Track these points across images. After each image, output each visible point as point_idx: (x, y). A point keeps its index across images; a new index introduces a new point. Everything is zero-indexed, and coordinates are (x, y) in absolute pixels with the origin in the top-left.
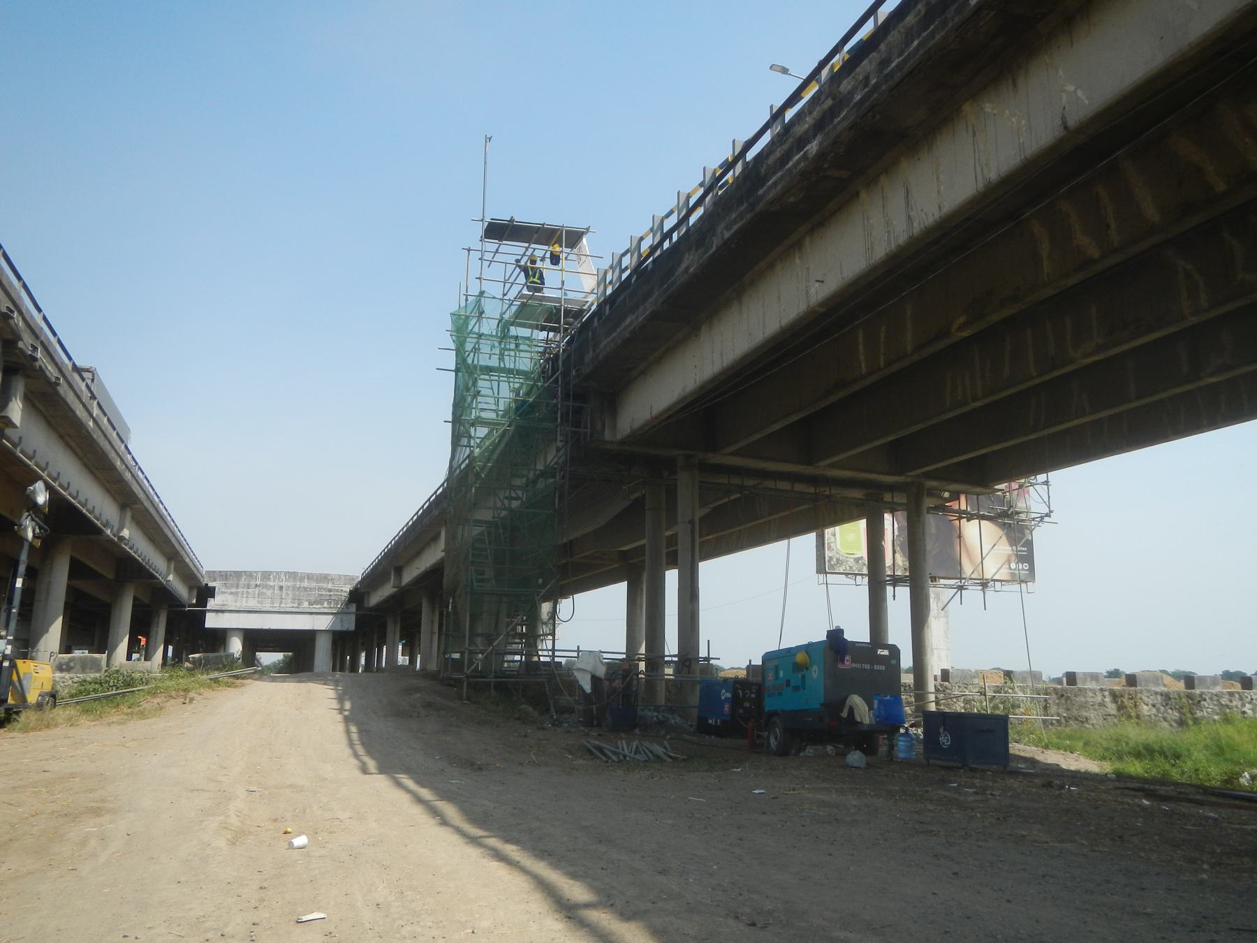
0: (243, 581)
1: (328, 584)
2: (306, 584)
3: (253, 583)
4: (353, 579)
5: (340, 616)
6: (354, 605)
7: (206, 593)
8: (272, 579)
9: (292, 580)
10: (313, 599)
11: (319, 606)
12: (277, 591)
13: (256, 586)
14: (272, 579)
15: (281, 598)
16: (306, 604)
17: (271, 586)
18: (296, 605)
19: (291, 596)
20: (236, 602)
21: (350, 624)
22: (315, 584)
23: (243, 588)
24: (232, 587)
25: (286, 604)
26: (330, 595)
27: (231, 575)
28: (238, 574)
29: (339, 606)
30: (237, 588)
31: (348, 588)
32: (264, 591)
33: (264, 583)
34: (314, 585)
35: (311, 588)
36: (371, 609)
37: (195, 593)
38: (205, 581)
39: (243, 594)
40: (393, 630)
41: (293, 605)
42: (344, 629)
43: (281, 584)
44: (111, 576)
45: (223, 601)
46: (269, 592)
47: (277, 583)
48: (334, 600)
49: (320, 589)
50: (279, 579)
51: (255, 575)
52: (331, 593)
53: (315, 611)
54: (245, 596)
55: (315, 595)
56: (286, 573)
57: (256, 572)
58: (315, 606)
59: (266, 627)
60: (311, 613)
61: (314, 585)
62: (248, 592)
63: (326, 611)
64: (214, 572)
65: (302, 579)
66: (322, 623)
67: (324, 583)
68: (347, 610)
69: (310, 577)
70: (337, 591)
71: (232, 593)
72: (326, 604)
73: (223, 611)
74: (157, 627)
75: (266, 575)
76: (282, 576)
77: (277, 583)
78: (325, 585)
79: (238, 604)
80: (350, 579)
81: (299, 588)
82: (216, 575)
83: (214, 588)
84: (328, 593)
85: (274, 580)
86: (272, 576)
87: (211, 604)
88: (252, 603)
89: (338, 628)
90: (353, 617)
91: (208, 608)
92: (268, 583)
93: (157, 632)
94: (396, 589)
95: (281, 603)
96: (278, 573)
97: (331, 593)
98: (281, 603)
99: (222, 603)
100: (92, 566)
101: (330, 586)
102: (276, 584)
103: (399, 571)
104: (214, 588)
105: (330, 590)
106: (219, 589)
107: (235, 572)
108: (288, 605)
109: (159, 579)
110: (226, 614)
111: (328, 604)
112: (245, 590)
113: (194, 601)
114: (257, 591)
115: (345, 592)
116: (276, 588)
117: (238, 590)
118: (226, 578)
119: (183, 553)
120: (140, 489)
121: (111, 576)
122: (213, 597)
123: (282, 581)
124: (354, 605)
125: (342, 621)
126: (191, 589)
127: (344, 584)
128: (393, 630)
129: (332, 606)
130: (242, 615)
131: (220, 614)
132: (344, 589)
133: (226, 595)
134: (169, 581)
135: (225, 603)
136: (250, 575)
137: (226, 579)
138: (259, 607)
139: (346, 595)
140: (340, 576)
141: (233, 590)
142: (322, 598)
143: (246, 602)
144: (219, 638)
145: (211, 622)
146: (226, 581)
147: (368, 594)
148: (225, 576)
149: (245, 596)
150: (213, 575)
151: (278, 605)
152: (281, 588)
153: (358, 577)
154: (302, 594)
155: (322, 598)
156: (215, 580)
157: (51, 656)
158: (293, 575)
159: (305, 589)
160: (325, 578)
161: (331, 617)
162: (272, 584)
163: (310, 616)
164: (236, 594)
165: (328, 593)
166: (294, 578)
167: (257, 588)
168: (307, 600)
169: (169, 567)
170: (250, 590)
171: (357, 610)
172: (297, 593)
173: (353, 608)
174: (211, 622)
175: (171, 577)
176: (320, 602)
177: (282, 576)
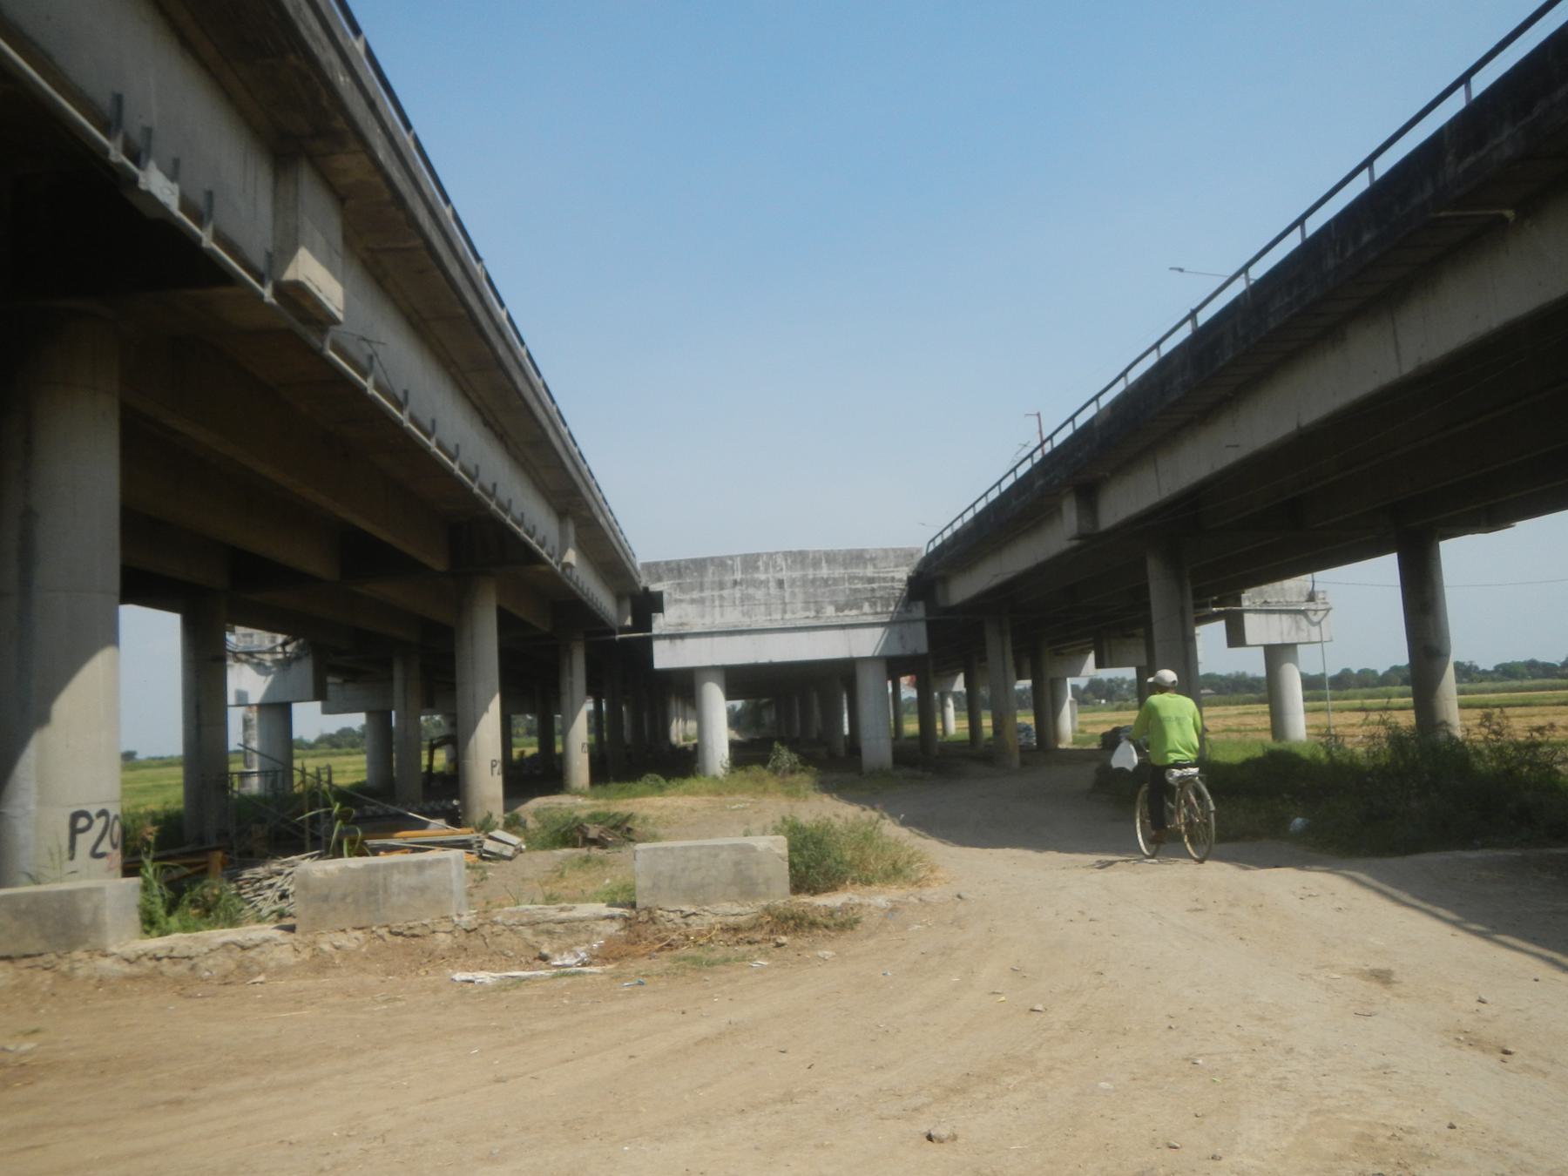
0: (710, 575)
1: (865, 568)
2: (824, 572)
3: (728, 578)
4: (912, 555)
5: (897, 628)
6: (921, 604)
7: (647, 605)
8: (762, 568)
9: (799, 566)
10: (841, 599)
11: (854, 612)
12: (773, 590)
13: (735, 583)
14: (762, 568)
15: (784, 604)
16: (830, 611)
17: (762, 582)
18: (812, 614)
19: (800, 597)
20: (703, 616)
21: (918, 642)
22: (842, 571)
23: (713, 589)
24: (693, 590)
25: (793, 613)
26: (873, 590)
27: (687, 568)
28: (699, 565)
29: (892, 609)
30: (702, 590)
31: (903, 573)
32: (751, 591)
33: (749, 576)
34: (839, 572)
35: (834, 579)
36: (952, 610)
37: (627, 606)
38: (644, 581)
39: (713, 601)
40: (999, 649)
41: (807, 614)
42: (908, 652)
43: (779, 576)
44: (440, 565)
45: (680, 617)
46: (759, 594)
47: (771, 576)
48: (881, 598)
49: (852, 578)
50: (774, 567)
51: (730, 562)
52: (875, 586)
53: (848, 621)
54: (717, 603)
55: (844, 591)
56: (787, 554)
57: (731, 558)
58: (847, 612)
59: (763, 659)
60: (843, 627)
61: (839, 572)
62: (721, 598)
63: (871, 619)
64: (656, 564)
65: (816, 564)
66: (866, 643)
67: (857, 566)
68: (909, 616)
69: (831, 558)
70: (885, 580)
71: (693, 601)
72: (866, 608)
73: (682, 636)
74: (571, 674)
75: (750, 562)
76: (780, 561)
77: (771, 576)
78: (859, 572)
79: (708, 620)
80: (904, 555)
81: (813, 581)
82: (660, 571)
83: (660, 594)
84: (869, 586)
85: (766, 570)
86: (760, 563)
87: (660, 623)
88: (733, 617)
89: (896, 650)
90: (922, 628)
91: (655, 631)
92: (756, 576)
93: (571, 683)
94: (1075, 543)
95: (784, 612)
96: (770, 555)
97: (875, 586)
98: (784, 612)
99: (679, 621)
101: (870, 571)
102: (770, 576)
103: (1088, 494)
104: (660, 594)
105: (871, 580)
106: (670, 594)
107: (694, 561)
108: (799, 616)
109: (550, 564)
110: (689, 642)
111: (871, 606)
112: (716, 593)
113: (629, 622)
114: (737, 593)
115: (900, 580)
116: (772, 584)
117: (703, 595)
118: (679, 571)
119: (584, 490)
120: (317, 27)
121: (440, 565)
123: (781, 569)
124: (921, 604)
125: (902, 637)
126: (619, 598)
127: (896, 566)
128: (999, 649)
129: (879, 610)
130: (717, 640)
131: (678, 642)
132: (898, 575)
133: (684, 605)
134: (569, 565)
135: (684, 620)
136: (721, 563)
137: (680, 575)
138: (745, 623)
139: (902, 586)
140: (885, 551)
141: (696, 595)
142: (859, 595)
143: (722, 615)
144: (684, 685)
145: (665, 657)
147: (945, 580)
148: (676, 570)
149: (717, 603)
150: (654, 569)
151: (778, 616)
152: (780, 583)
153: (919, 550)
154: (820, 591)
155: (859, 595)
156: (659, 579)
157: (74, 832)
158: (799, 558)
159: (825, 581)
160: (858, 557)
161: (879, 631)
162: (762, 577)
163: (842, 632)
164: (702, 601)
165: (869, 586)
166: (803, 562)
167: (738, 588)
168: (831, 603)
169: (563, 534)
170: (725, 593)
171: (927, 615)
172: (812, 590)
173: (919, 611)
174: (665, 657)
175: (571, 556)
176: (849, 605)
177: (780, 561)
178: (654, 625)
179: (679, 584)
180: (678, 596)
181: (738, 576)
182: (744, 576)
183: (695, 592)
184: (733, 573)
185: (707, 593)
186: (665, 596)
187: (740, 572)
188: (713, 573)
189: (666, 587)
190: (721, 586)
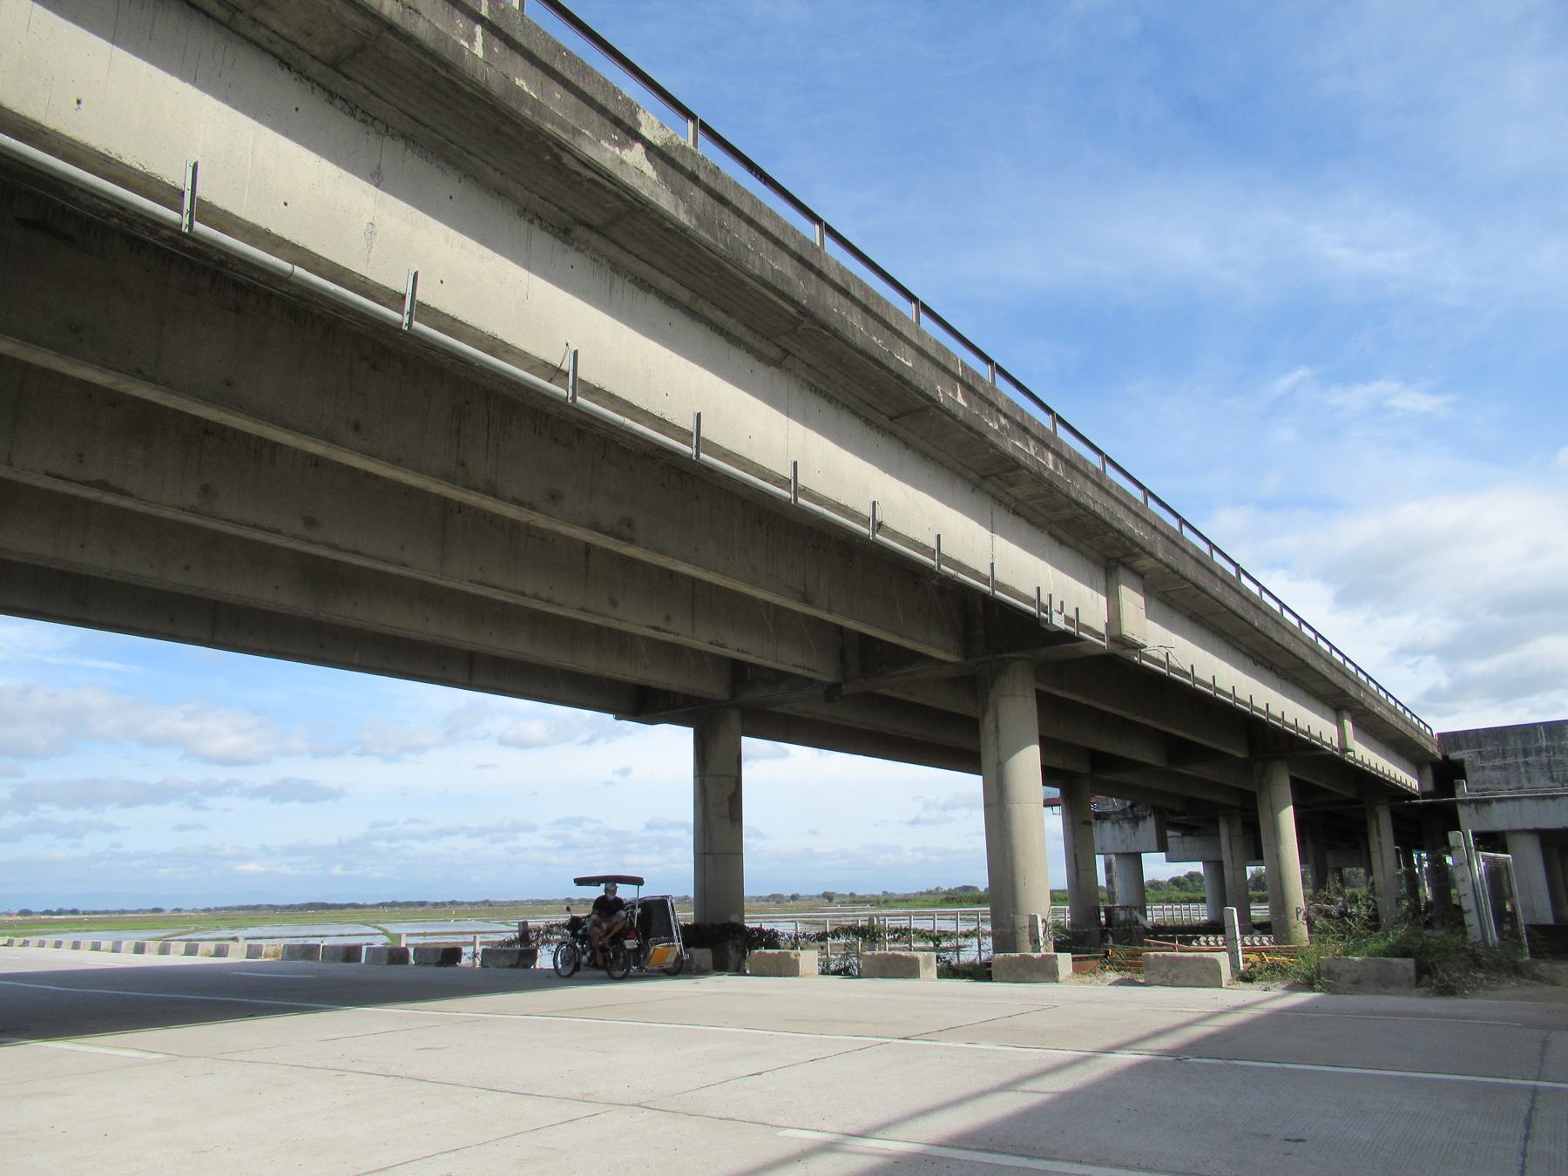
13: (1539, 751)
30: (1504, 757)
37: (1428, 773)
39: (1518, 769)
54: (1522, 770)
62: (1527, 764)
71: (1494, 768)
83: (1461, 762)
87: (1463, 790)
100: (443, 583)
117: (1506, 762)
122: (1463, 776)
141: (1498, 762)
146: (1479, 747)
149: (1522, 770)
156: (1458, 748)
164: (1505, 768)
170: (1531, 759)
178: (1457, 791)
179: (1480, 752)
180: (1479, 763)
181: (1544, 743)
182: (1549, 744)
183: (1496, 760)
184: (1538, 739)
185: (1510, 760)
186: (1467, 765)
187: (1544, 740)
188: (1515, 742)
189: (1467, 755)
190: (1526, 753)
